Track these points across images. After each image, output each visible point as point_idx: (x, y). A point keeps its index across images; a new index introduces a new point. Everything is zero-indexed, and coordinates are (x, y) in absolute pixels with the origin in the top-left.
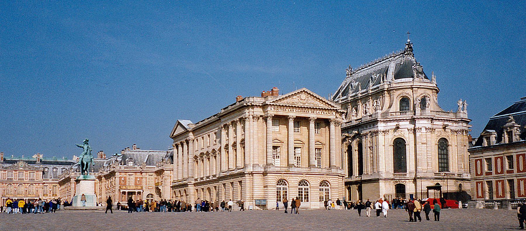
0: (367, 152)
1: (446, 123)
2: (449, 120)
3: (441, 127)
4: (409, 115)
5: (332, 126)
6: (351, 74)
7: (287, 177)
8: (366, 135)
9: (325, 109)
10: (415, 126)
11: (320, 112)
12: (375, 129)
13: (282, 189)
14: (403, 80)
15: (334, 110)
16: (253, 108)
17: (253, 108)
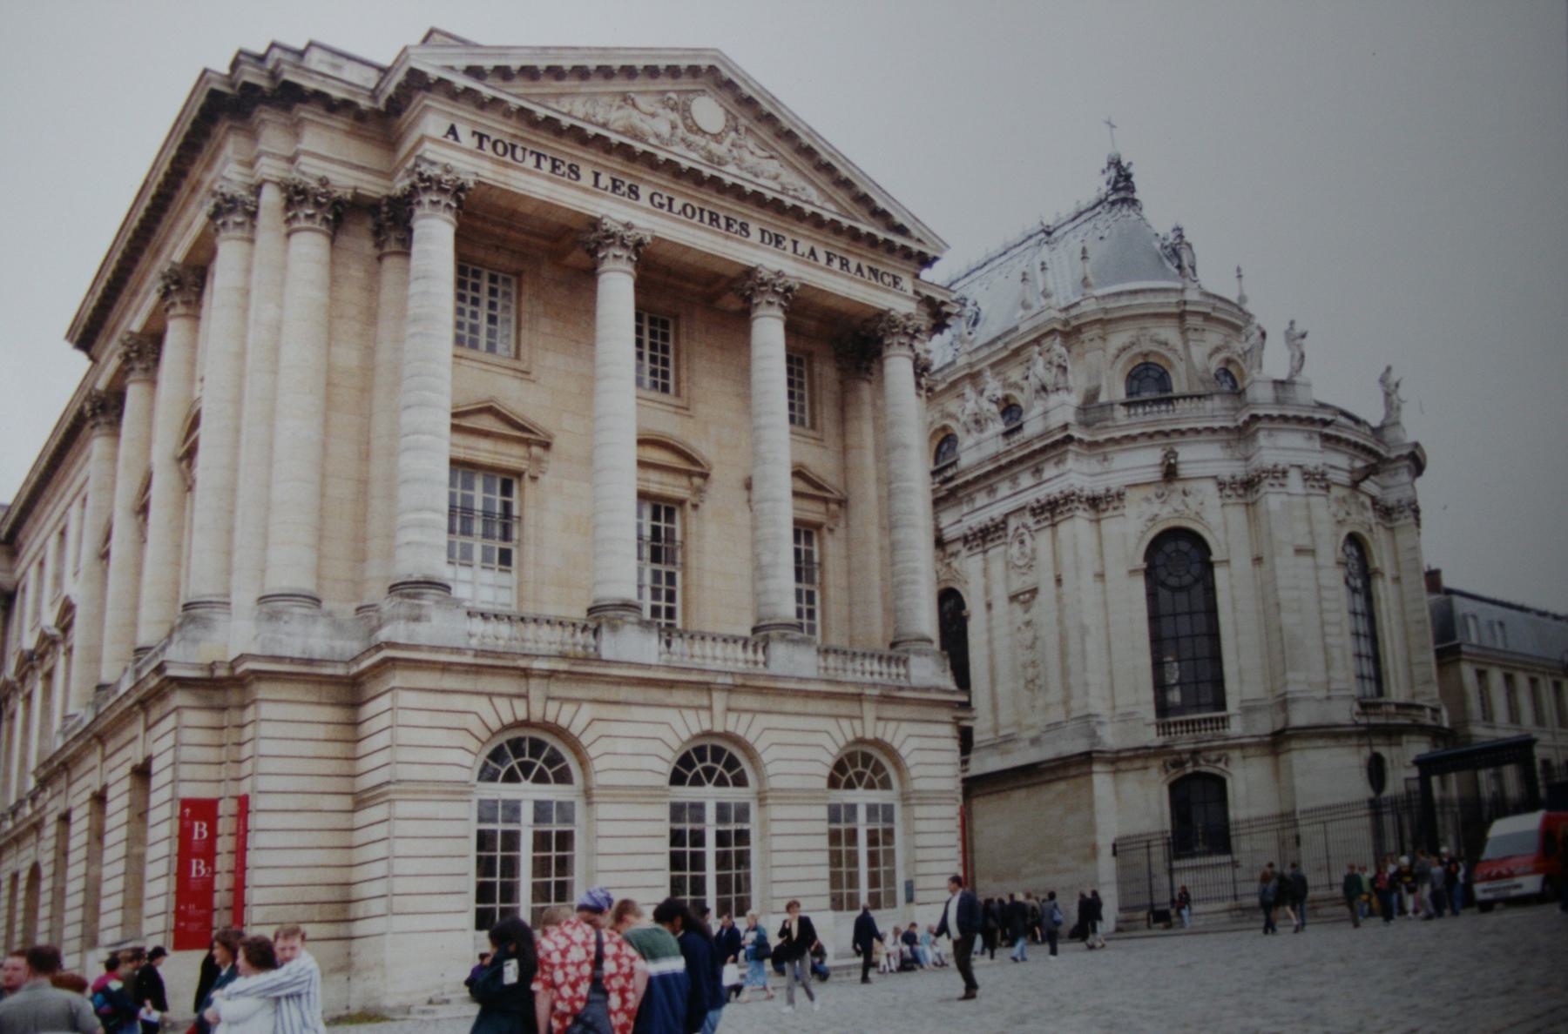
3: (1344, 478)
8: (985, 536)
9: (854, 235)
13: (527, 813)
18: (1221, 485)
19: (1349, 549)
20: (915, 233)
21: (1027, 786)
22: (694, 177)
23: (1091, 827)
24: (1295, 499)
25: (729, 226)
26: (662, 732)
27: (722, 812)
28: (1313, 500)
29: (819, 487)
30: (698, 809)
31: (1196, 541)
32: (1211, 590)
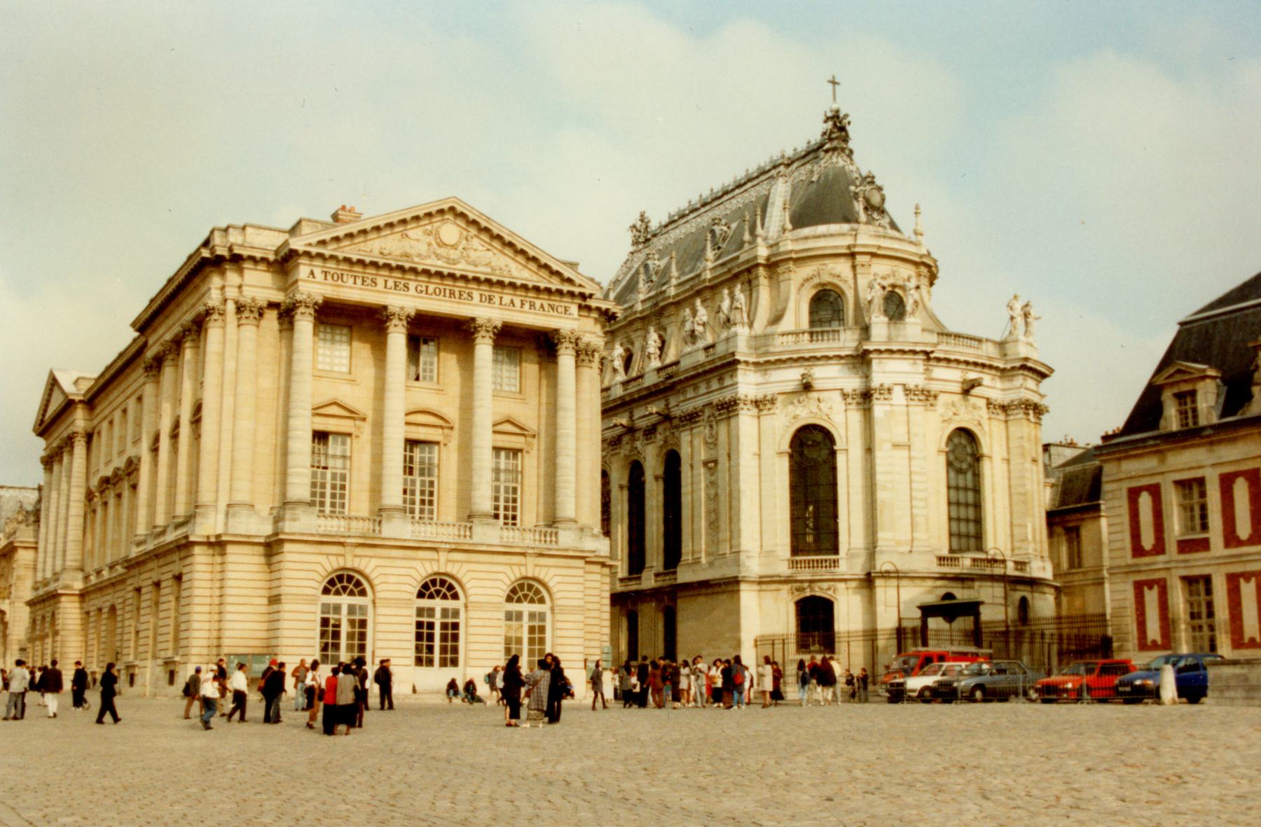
0: (694, 484)
1: (972, 375)
2: (983, 366)
3: (957, 388)
4: (847, 341)
5: (566, 360)
6: (647, 240)
7: (367, 563)
8: (691, 418)
9: (537, 289)
10: (867, 377)
11: (517, 301)
12: (727, 395)
13: (344, 610)
14: (821, 229)
15: (572, 294)
16: (241, 271)
17: (241, 271)
18: (845, 396)
19: (956, 440)
20: (578, 282)
21: (707, 595)
22: (440, 275)
23: (737, 627)
24: (896, 409)
25: (460, 295)
26: (412, 572)
27: (445, 612)
28: (911, 409)
29: (522, 428)
30: (431, 612)
31: (828, 437)
32: (834, 469)
